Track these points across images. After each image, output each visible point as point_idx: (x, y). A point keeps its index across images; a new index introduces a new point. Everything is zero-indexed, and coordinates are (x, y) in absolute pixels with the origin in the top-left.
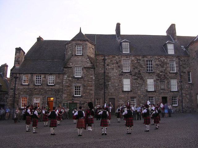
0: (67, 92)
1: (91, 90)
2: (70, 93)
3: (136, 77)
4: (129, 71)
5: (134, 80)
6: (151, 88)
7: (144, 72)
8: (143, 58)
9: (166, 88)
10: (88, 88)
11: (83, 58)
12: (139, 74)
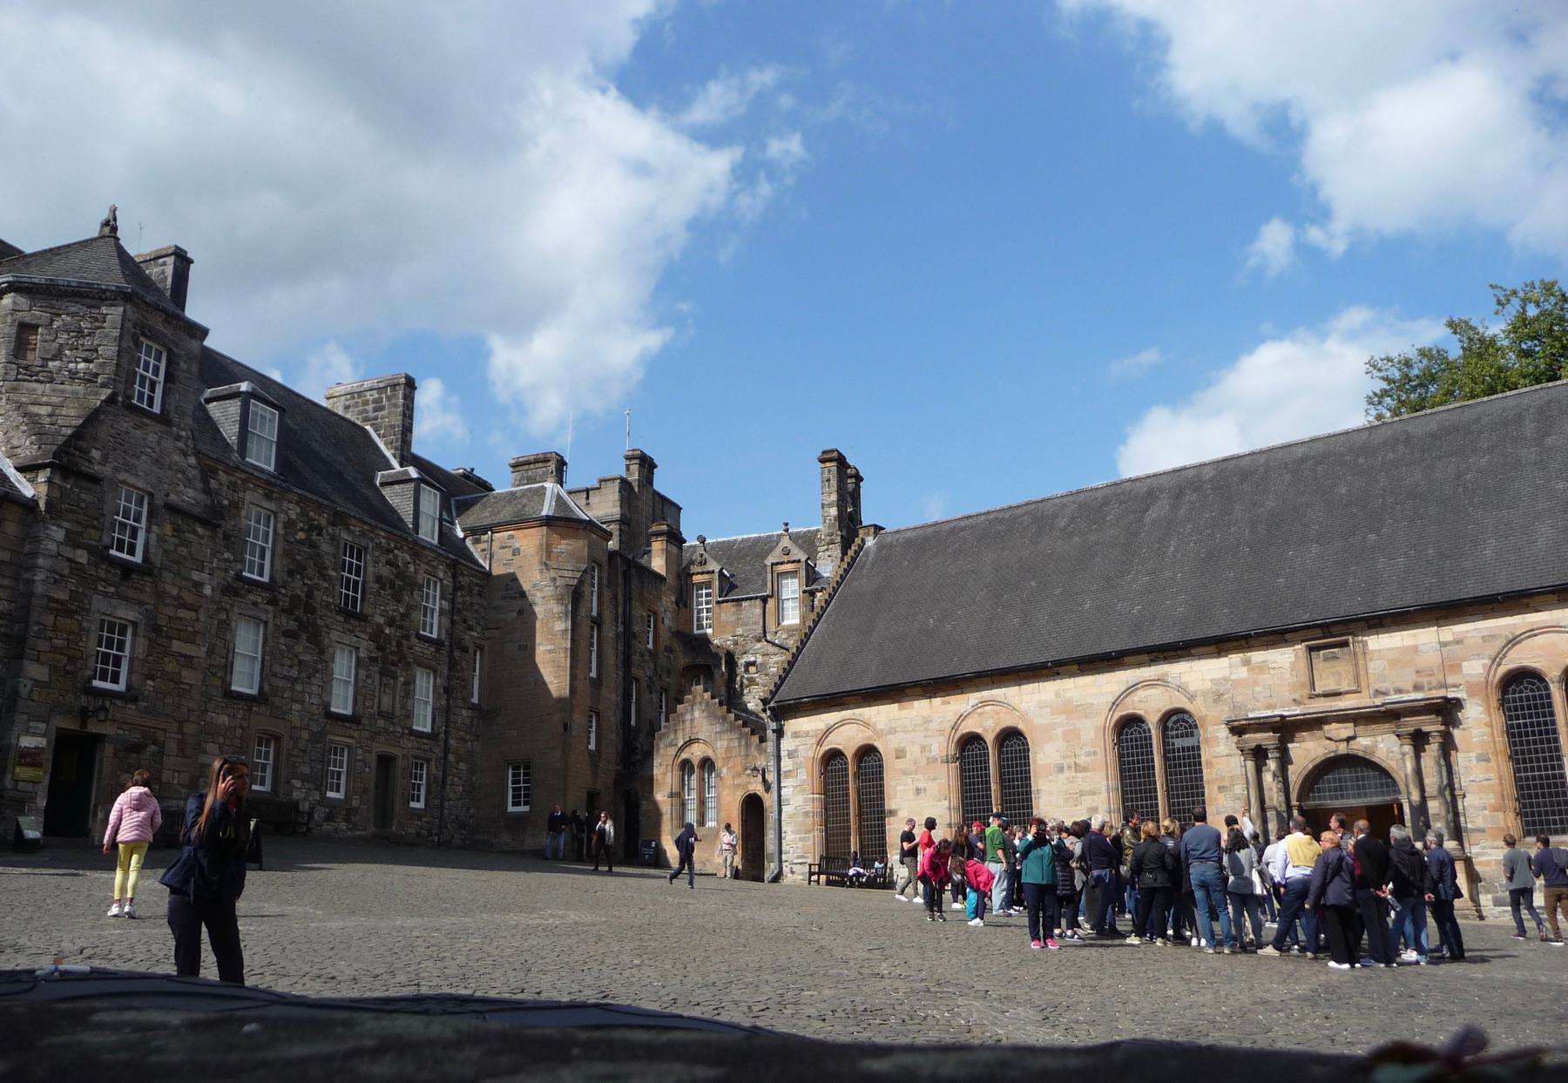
0: (55, 650)
1: (189, 661)
2: (72, 660)
3: (293, 625)
4: (266, 579)
5: (282, 640)
6: (342, 703)
7: (328, 606)
8: (333, 524)
9: (398, 711)
10: (177, 646)
11: (168, 444)
12: (306, 612)
